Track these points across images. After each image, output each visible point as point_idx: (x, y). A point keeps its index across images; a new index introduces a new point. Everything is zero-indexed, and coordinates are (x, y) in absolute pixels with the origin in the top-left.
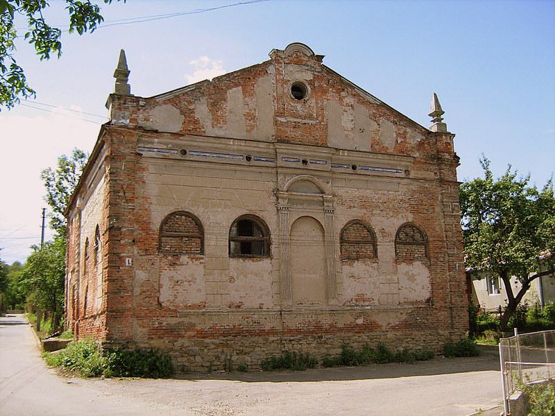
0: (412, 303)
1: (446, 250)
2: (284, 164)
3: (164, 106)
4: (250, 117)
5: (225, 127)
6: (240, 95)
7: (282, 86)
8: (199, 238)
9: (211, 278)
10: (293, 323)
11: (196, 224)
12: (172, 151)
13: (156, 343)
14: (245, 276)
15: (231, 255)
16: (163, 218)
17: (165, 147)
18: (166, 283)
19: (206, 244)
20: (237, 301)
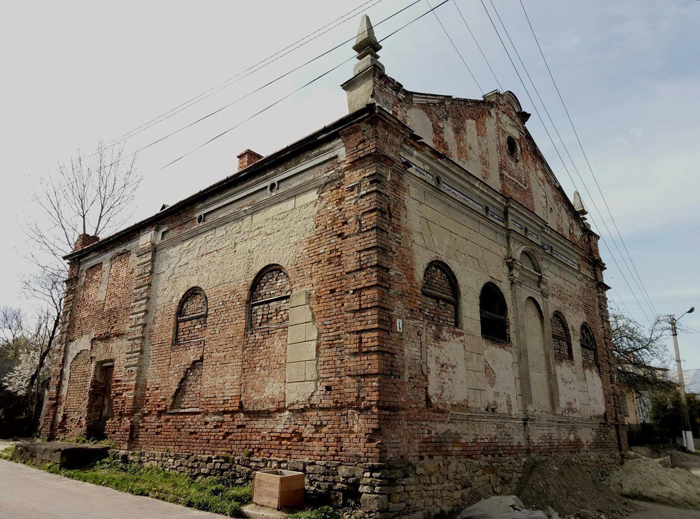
12: (428, 175)
18: (433, 366)
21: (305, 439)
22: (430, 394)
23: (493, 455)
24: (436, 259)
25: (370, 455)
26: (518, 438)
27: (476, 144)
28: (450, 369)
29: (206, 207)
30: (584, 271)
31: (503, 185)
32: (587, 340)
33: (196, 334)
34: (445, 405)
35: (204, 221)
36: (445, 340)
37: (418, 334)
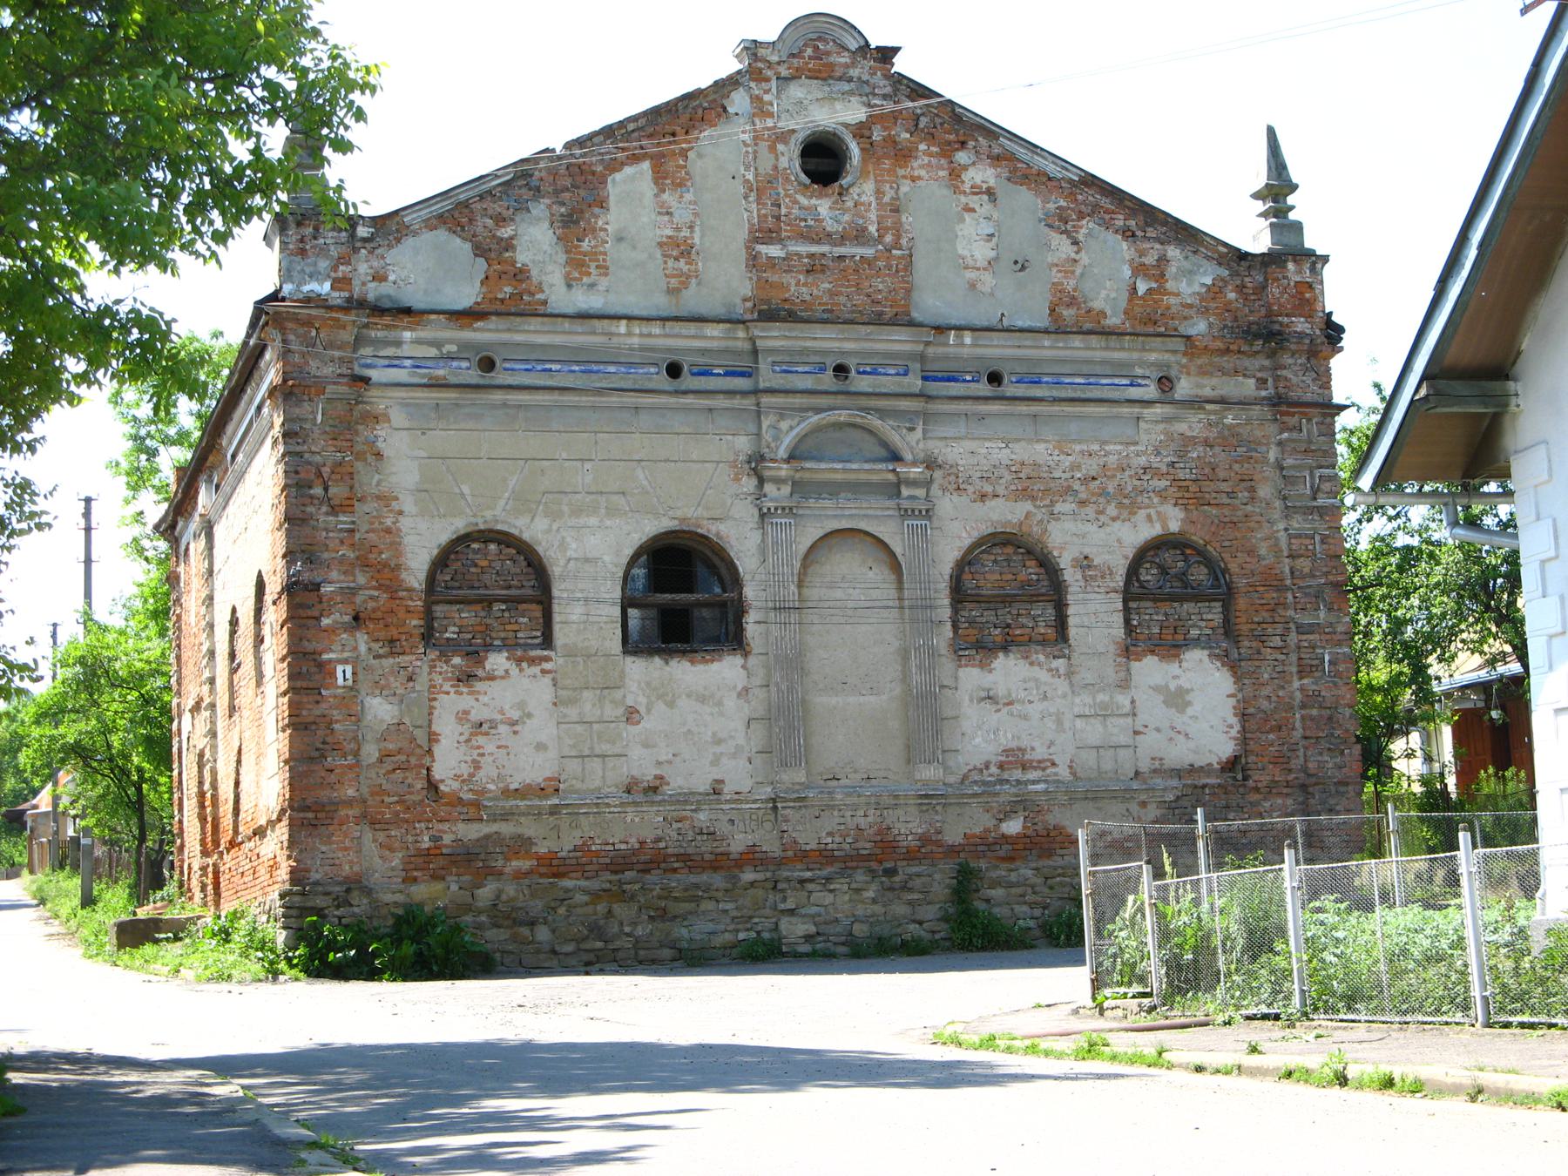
0: (1178, 773)
1: (1291, 613)
2: (778, 381)
3: (428, 236)
4: (679, 248)
5: (603, 283)
6: (646, 186)
7: (772, 149)
8: (539, 602)
9: (572, 713)
10: (810, 833)
11: (529, 565)
12: (455, 364)
13: (426, 892)
14: (671, 704)
15: (632, 646)
16: (435, 552)
17: (433, 352)
18: (447, 728)
19: (557, 618)
20: (648, 773)
28: (503, 729)
31: (763, 284)
34: (484, 791)
36: (491, 678)
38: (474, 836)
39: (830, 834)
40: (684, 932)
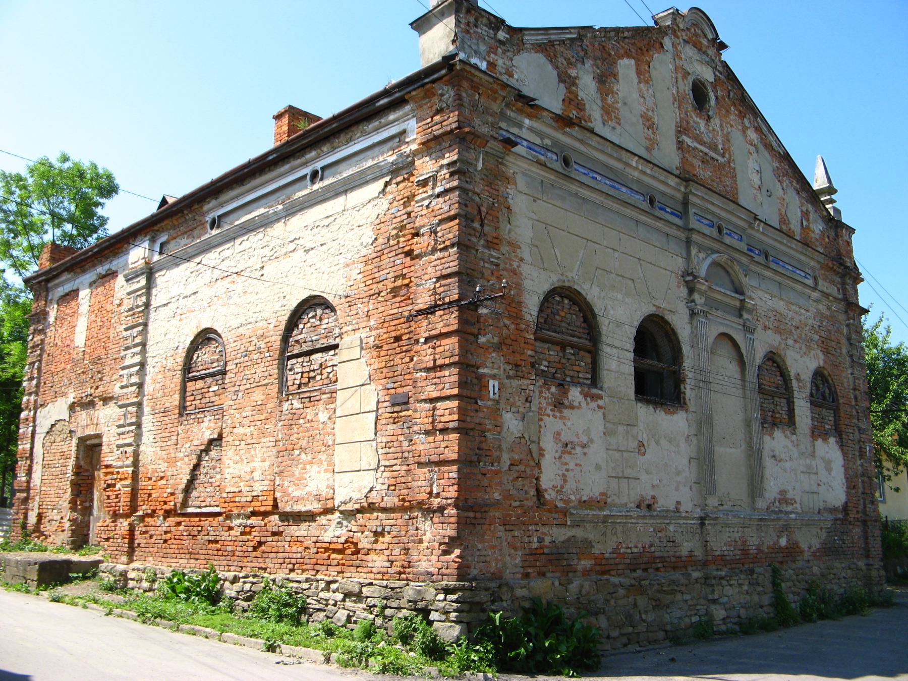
1: (855, 421)
8: (589, 352)
11: (585, 321)
12: (550, 154)
13: (544, 587)
18: (549, 446)
21: (362, 552)
22: (544, 487)
23: (645, 570)
24: (561, 284)
25: (444, 571)
26: (688, 546)
27: (635, 95)
28: (578, 450)
29: (221, 205)
30: (823, 285)
31: (684, 160)
32: (823, 395)
33: (212, 399)
34: (567, 502)
35: (218, 227)
36: (572, 407)
37: (527, 400)
38: (562, 539)
39: (725, 544)
40: (667, 616)
